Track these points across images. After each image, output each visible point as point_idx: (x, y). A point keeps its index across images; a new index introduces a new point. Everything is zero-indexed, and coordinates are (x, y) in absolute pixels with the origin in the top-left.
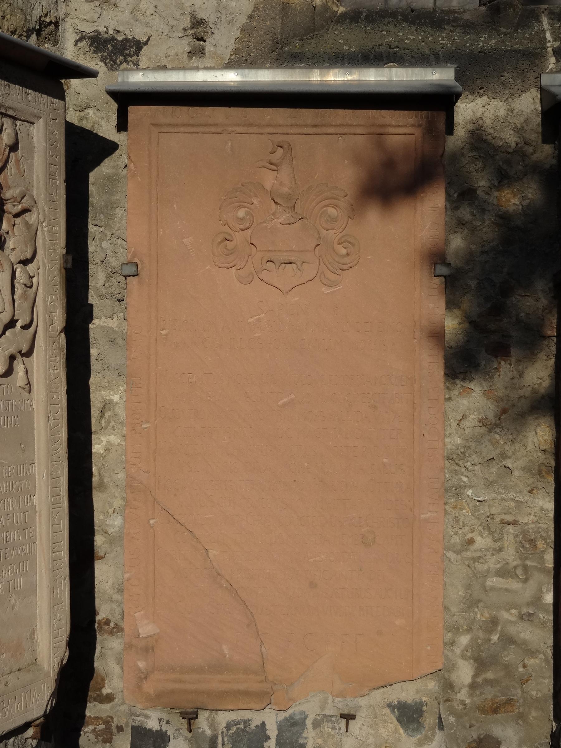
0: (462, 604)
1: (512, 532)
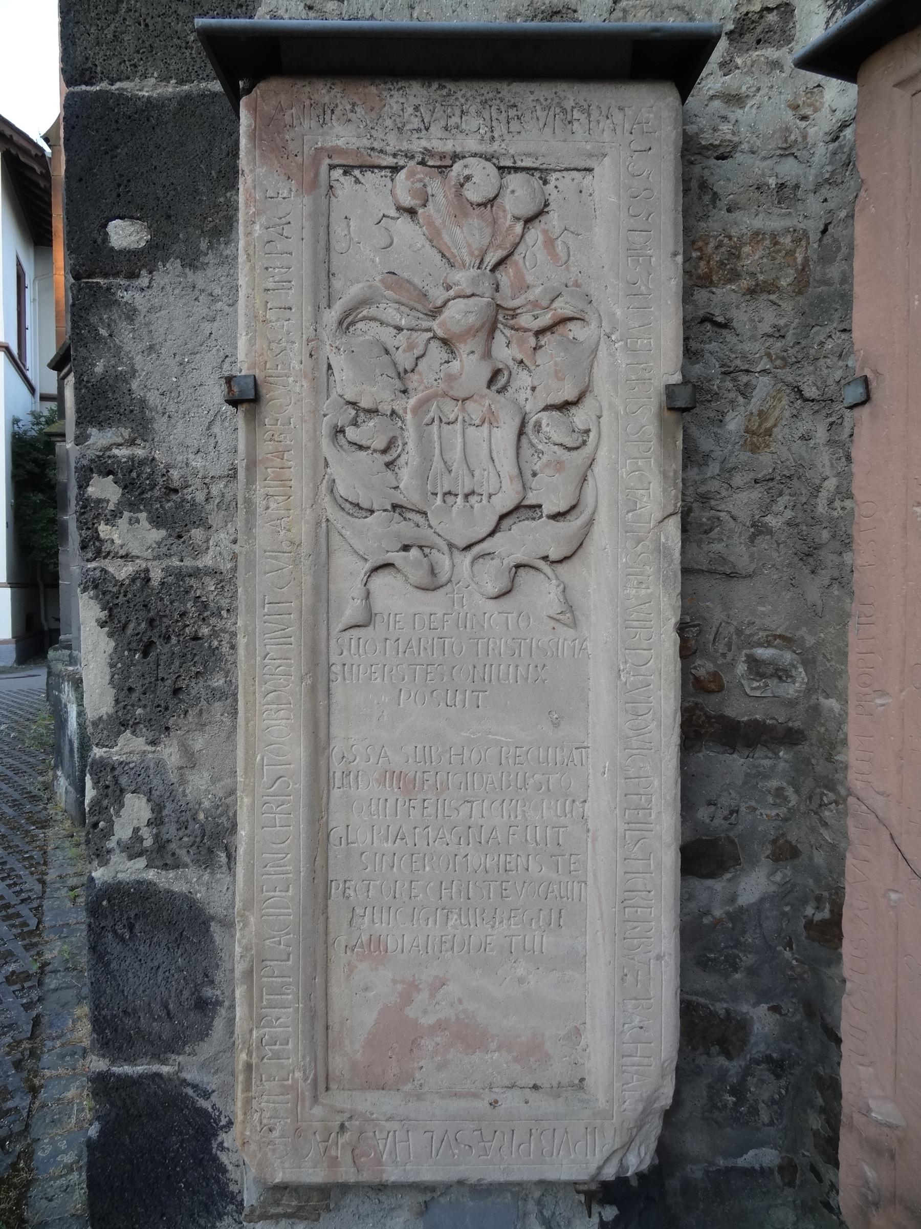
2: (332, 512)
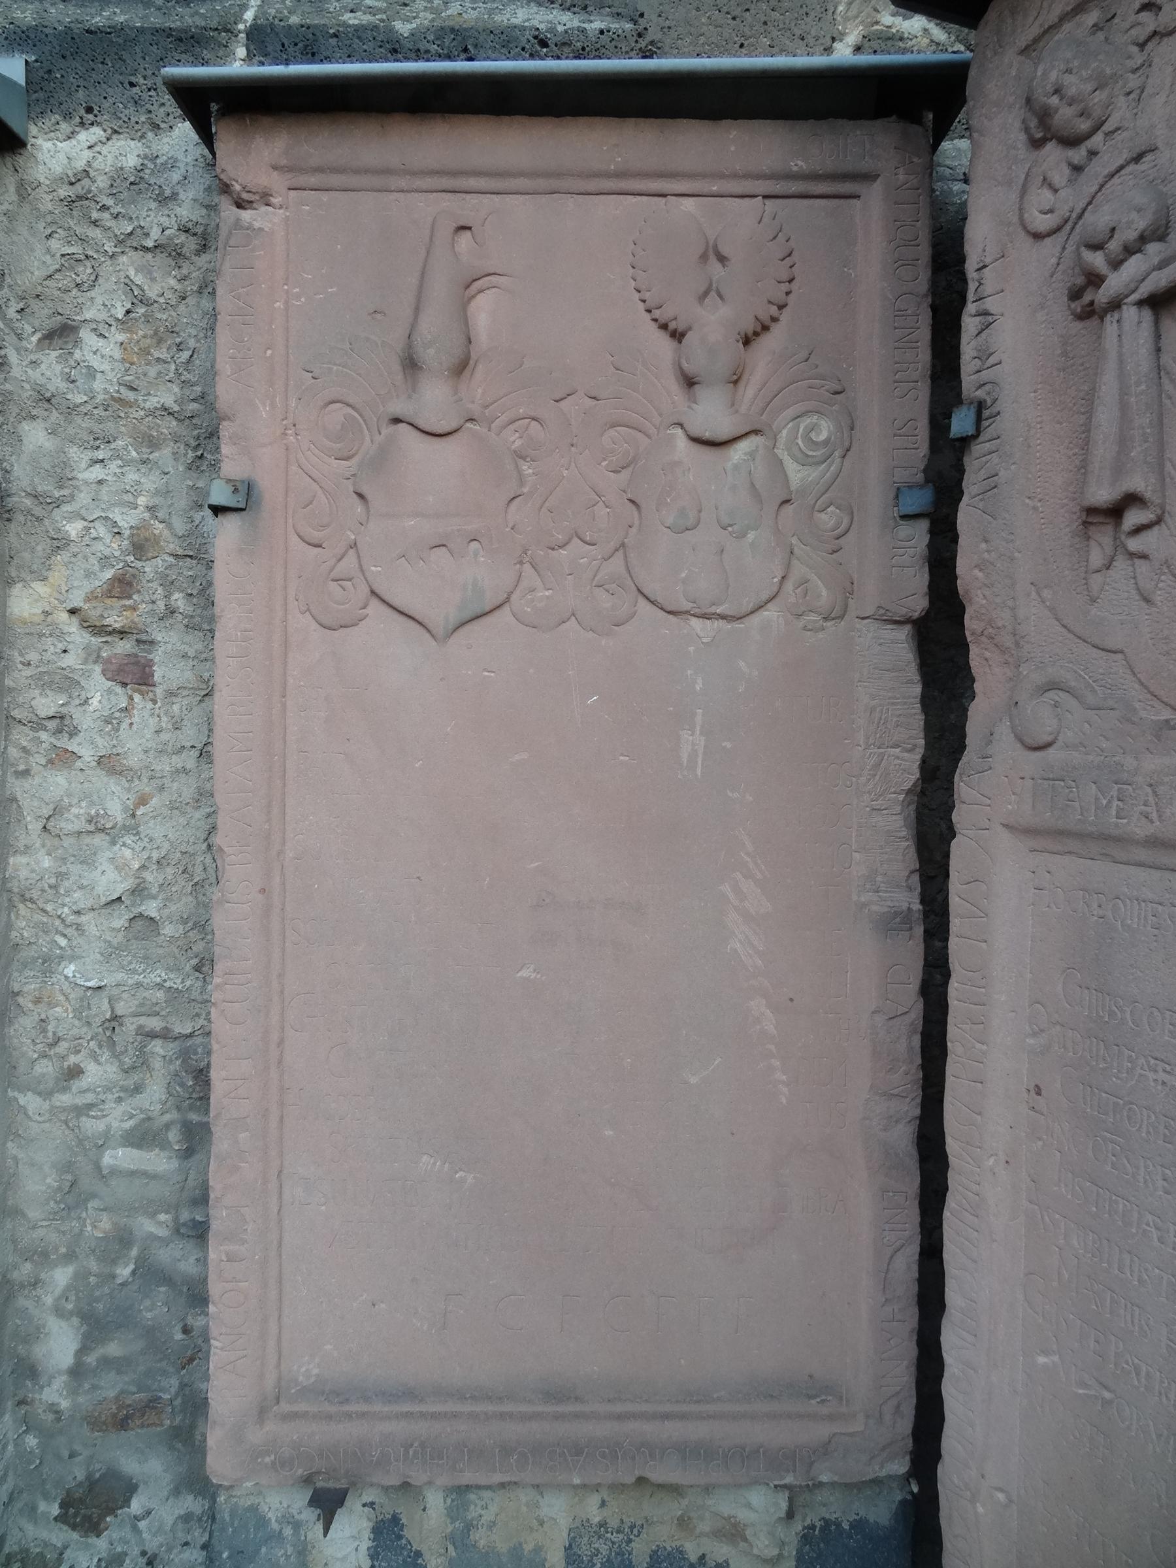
0: (52, 1203)
1: (162, 1052)
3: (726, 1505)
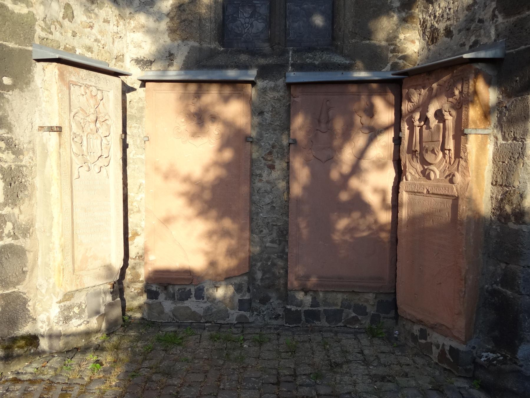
2: (73, 155)
3: (366, 296)
